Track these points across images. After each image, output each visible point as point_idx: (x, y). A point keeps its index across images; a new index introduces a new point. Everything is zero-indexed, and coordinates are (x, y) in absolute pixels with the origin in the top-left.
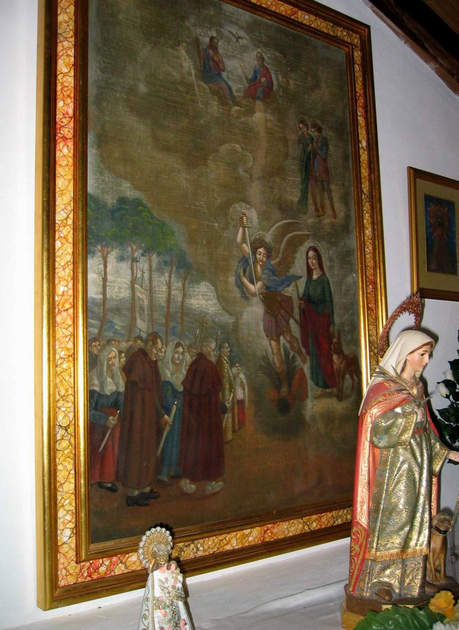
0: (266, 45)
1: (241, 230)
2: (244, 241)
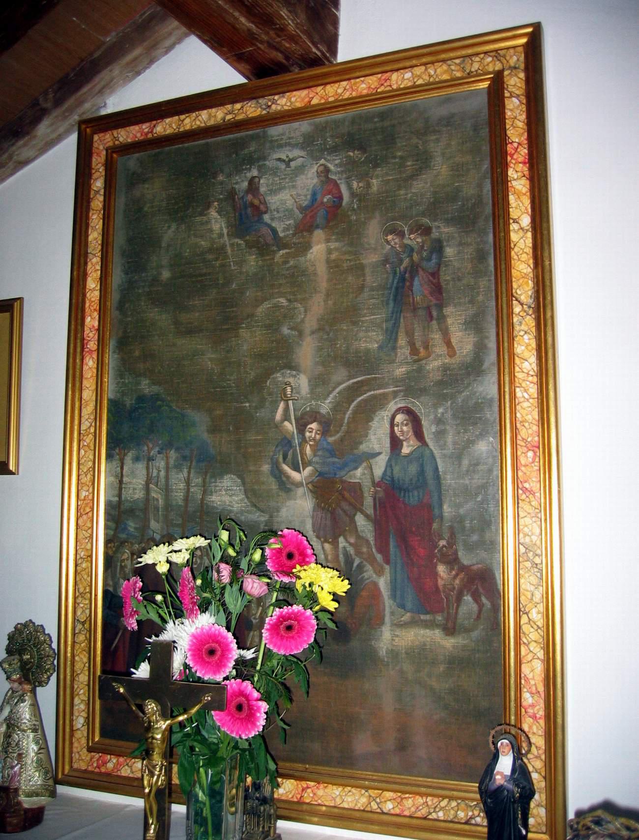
1: (282, 405)
2: (286, 417)
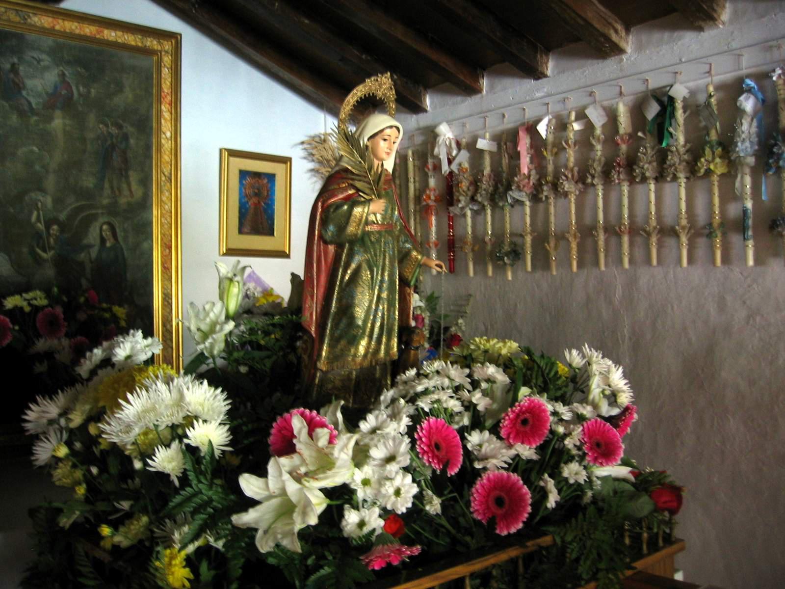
0: (68, 63)
1: (35, 214)
2: (38, 219)
